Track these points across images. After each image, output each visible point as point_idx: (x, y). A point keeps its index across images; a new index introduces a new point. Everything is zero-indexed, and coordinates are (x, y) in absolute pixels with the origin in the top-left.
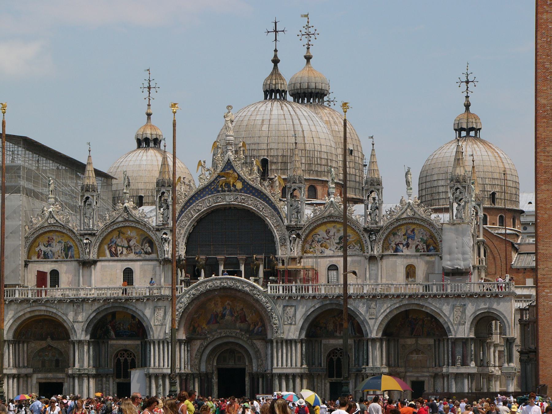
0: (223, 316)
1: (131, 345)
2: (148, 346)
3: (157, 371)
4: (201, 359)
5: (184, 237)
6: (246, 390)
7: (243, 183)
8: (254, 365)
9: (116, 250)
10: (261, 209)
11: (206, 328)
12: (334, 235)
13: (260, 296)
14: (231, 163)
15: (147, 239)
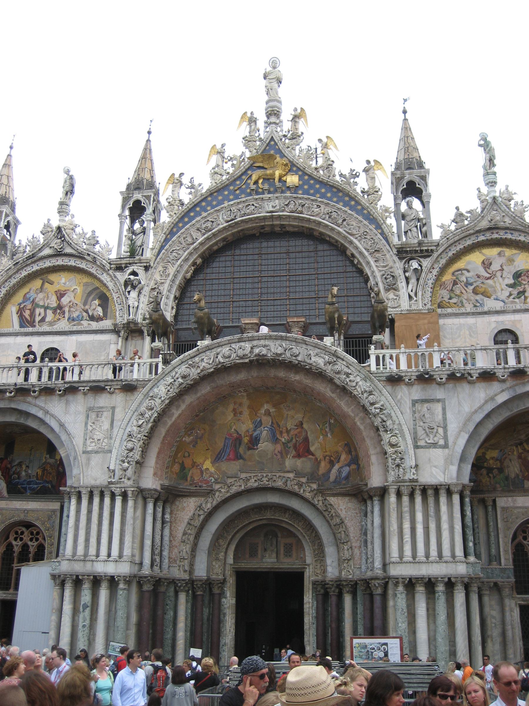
0: (254, 442)
1: (37, 510)
2: (66, 505)
3: (78, 568)
4: (195, 546)
5: (173, 281)
6: (306, 627)
7: (299, 176)
8: (329, 561)
9: (32, 314)
10: (340, 221)
11: (212, 470)
12: (502, 270)
13: (352, 377)
14: (276, 144)
15: (98, 291)
